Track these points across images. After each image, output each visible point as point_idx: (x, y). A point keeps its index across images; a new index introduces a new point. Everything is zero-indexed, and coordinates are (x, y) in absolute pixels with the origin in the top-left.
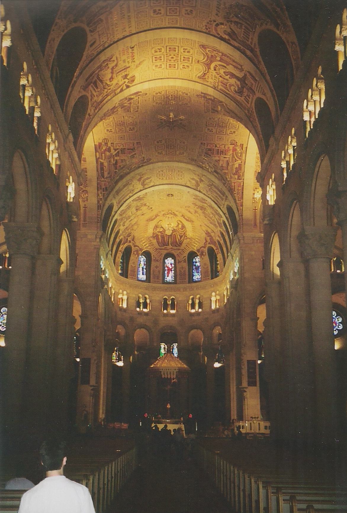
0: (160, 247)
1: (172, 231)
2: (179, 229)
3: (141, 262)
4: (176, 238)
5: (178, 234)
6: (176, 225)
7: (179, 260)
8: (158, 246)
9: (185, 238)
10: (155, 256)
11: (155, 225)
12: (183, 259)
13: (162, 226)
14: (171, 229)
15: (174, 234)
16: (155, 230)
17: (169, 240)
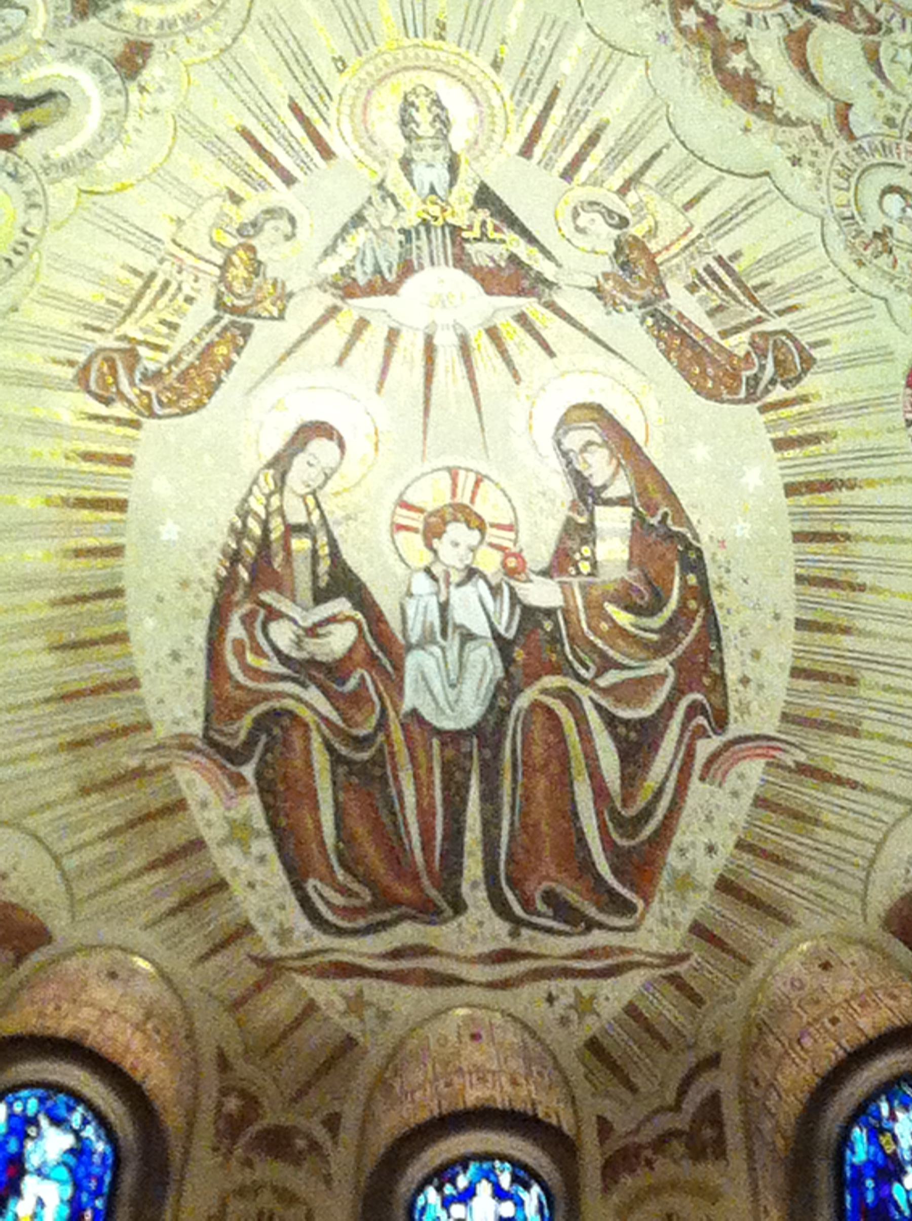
0: (322, 940)
1: (503, 646)
2: (595, 608)
3: (30, 1185)
4: (565, 782)
5: (584, 693)
6: (552, 529)
7: (622, 1123)
8: (304, 924)
9: (705, 748)
10: (243, 1069)
11: (228, 516)
12: (677, 1107)
13: (351, 556)
14: (481, 627)
15: (536, 705)
16: (236, 630)
17: (455, 833)
